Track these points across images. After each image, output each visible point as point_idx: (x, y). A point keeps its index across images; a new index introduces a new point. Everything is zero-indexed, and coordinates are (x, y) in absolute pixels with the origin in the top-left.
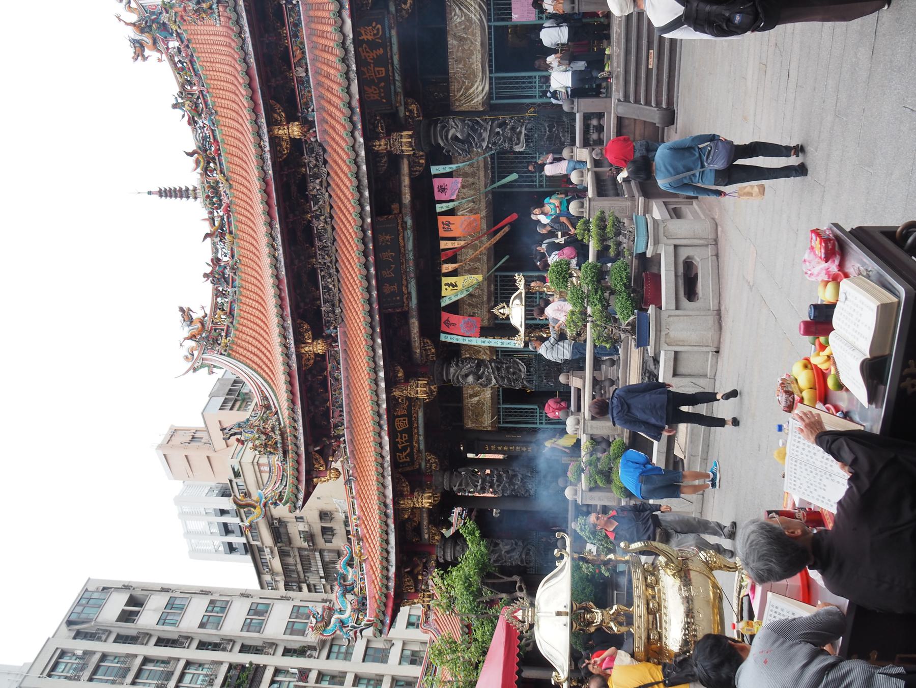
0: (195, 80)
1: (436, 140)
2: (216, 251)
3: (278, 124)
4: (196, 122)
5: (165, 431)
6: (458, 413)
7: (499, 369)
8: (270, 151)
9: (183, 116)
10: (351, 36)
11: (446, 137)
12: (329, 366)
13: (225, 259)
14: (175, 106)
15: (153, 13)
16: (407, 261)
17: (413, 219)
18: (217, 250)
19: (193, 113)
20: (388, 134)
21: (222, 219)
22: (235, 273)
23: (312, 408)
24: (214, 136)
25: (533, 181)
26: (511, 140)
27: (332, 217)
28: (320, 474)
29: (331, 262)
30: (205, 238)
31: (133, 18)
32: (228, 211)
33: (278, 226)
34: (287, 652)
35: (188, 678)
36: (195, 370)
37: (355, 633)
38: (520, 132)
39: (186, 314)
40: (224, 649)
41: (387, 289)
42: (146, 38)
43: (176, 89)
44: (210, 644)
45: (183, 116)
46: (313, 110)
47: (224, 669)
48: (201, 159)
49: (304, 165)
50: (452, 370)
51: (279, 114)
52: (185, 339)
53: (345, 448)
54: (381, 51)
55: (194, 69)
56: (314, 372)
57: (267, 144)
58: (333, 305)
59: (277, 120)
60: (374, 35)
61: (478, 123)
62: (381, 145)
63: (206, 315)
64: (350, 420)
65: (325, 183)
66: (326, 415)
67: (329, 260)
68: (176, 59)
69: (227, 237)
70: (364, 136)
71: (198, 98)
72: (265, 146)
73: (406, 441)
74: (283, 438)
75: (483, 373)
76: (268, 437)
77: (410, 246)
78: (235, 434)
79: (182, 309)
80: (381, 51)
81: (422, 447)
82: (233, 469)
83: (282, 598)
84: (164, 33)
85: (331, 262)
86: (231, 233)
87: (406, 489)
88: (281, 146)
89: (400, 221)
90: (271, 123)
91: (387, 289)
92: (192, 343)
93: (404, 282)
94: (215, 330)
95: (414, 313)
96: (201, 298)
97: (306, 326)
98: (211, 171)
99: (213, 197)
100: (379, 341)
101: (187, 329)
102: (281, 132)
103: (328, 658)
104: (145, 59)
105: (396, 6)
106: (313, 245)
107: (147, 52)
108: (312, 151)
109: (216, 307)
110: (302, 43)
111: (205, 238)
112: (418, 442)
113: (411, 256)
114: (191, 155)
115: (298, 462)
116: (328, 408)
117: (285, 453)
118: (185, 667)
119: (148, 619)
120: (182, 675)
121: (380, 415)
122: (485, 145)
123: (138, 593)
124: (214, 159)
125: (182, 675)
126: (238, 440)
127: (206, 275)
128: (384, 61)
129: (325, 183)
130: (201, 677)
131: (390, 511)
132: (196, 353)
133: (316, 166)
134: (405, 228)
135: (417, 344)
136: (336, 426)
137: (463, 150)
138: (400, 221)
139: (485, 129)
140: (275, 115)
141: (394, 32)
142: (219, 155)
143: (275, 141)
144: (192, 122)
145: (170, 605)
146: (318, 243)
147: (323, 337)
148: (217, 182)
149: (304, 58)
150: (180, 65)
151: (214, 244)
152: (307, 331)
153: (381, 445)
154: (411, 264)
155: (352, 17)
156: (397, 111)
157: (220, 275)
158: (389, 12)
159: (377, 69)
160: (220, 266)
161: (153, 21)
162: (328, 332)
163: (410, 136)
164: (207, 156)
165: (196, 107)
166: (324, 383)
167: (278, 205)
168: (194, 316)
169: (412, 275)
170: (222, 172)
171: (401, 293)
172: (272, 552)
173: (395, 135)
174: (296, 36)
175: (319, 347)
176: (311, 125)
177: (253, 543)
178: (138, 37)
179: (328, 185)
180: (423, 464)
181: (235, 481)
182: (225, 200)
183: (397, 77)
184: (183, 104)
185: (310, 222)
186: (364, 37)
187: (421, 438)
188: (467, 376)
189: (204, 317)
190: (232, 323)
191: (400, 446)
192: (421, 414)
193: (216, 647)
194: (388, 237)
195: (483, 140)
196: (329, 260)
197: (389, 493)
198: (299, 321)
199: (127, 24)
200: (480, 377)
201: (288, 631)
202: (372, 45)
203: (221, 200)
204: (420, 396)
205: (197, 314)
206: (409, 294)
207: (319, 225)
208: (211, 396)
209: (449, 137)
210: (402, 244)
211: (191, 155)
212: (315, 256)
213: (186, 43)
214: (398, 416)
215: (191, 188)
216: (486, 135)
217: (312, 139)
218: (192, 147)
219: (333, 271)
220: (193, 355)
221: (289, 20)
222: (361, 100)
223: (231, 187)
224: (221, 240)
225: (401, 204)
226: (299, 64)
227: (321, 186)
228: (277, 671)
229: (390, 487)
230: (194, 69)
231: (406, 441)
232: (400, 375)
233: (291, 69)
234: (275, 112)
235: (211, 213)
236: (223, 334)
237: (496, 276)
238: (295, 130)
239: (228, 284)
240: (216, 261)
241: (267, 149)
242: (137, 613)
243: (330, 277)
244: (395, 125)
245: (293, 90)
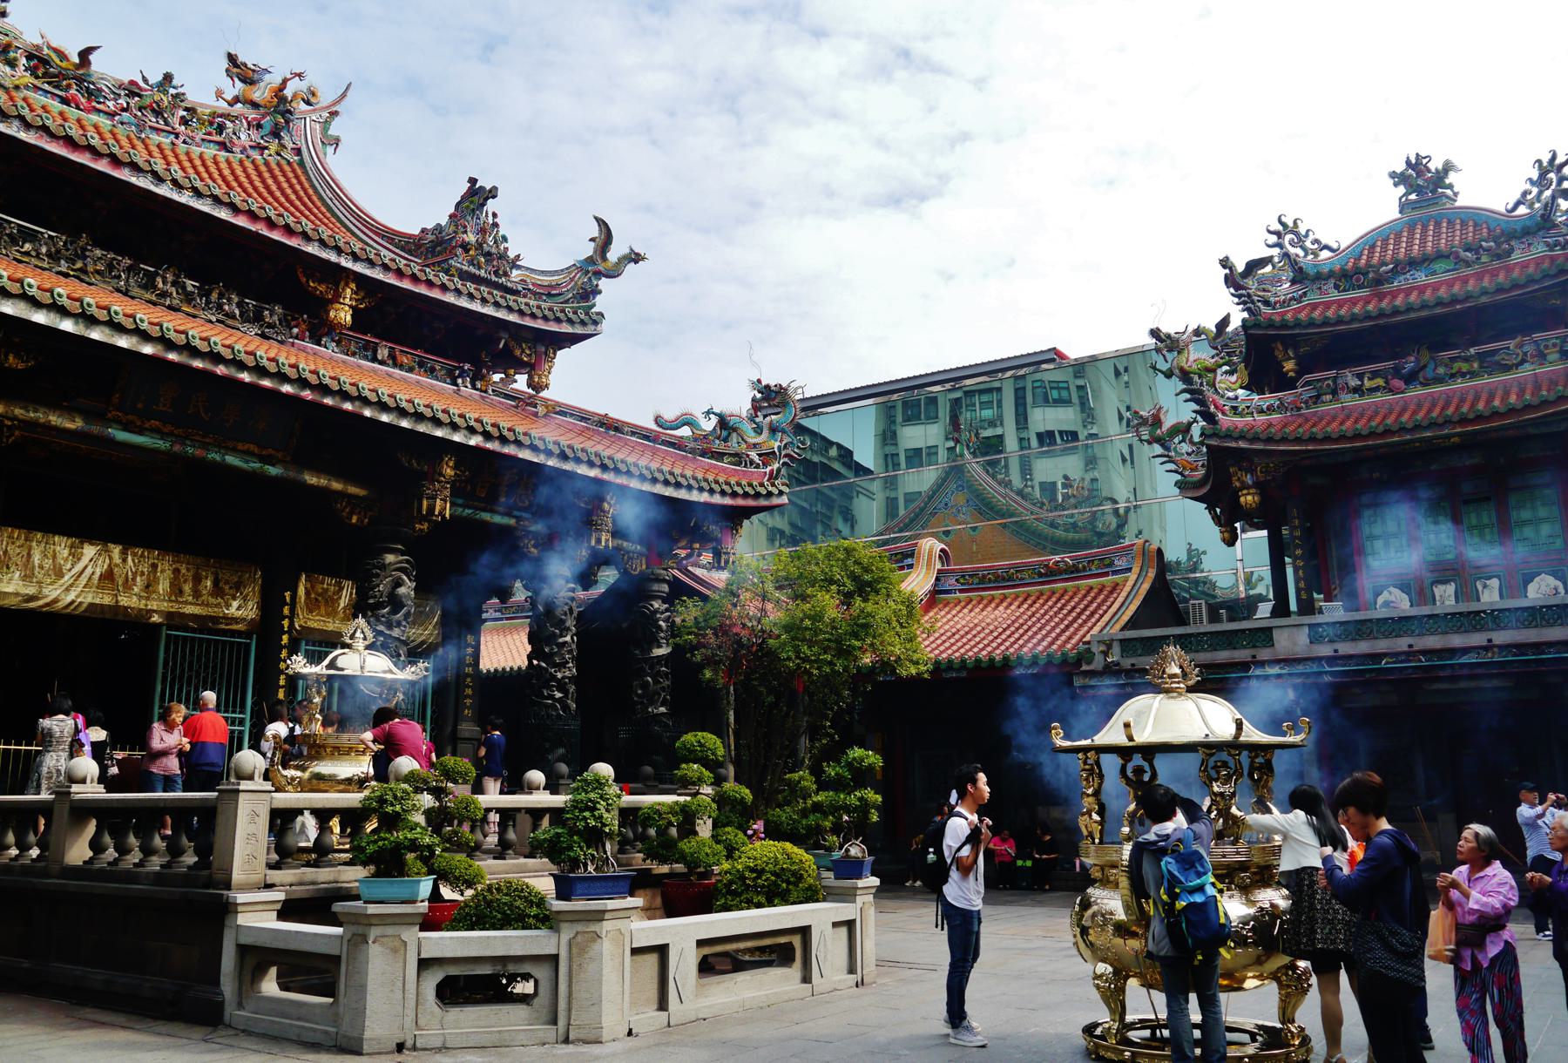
4: (131, 94)
8: (338, 266)
14: (168, 78)
16: (205, 446)
17: (276, 479)
19: (148, 101)
24: (99, 111)
25: (234, 706)
31: (288, 93)
45: (145, 80)
48: (64, 64)
67: (90, 268)
68: (229, 124)
70: (476, 448)
71: (167, 124)
77: (231, 459)
89: (279, 455)
90: (361, 279)
95: (95, 429)
100: (148, 349)
107: (239, 84)
110: (411, 370)
113: (214, 456)
114: (85, 54)
129: (230, 322)
135: (18, 412)
138: (279, 455)
141: (512, 522)
142: (65, 101)
143: (337, 275)
144: (132, 90)
148: (12, 64)
149: (395, 365)
154: (198, 452)
161: (287, 122)
165: (153, 110)
167: (256, 233)
169: (177, 448)
174: (421, 364)
184: (166, 92)
195: (390, 627)
199: (285, 81)
206: (140, 432)
210: (240, 446)
211: (85, 54)
213: (251, 152)
217: (295, 330)
218: (97, 63)
226: (392, 356)
227: (226, 315)
243: (49, 255)
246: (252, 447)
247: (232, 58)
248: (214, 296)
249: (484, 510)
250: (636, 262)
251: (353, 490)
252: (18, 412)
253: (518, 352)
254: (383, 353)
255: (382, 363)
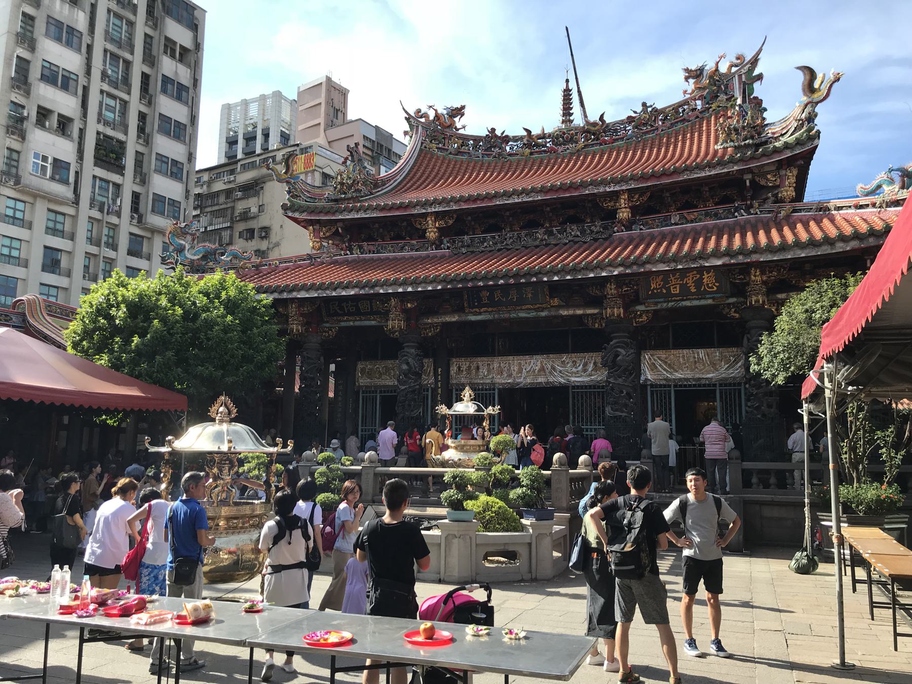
0: (668, 123)
1: (616, 338)
2: (515, 139)
3: (630, 199)
5: (344, 84)
6: (372, 356)
7: (413, 391)
9: (635, 112)
10: (707, 265)
11: (618, 347)
12: (414, 242)
13: (508, 148)
14: (644, 104)
15: (727, 86)
17: (546, 317)
18: (516, 141)
20: (621, 296)
21: (545, 146)
22: (495, 157)
23: (377, 226)
24: (617, 140)
26: (616, 403)
27: (547, 245)
28: (315, 233)
29: (507, 245)
30: (526, 130)
31: (723, 69)
32: (551, 150)
33: (540, 198)
34: (136, 197)
35: (112, 102)
36: (407, 119)
37: (172, 263)
38: (622, 412)
39: (458, 112)
40: (139, 137)
41: (485, 294)
42: (705, 81)
43: (659, 107)
44: (144, 123)
45: (635, 112)
46: (641, 229)
47: (121, 137)
49: (592, 221)
50: (413, 350)
51: (638, 200)
52: (436, 111)
53: (341, 255)
54: (693, 290)
55: (677, 122)
56: (409, 228)
57: (612, 189)
58: (468, 246)
59: (633, 197)
60: (708, 284)
61: (631, 374)
62: (611, 289)
63: (457, 130)
64: (365, 261)
65: (577, 239)
66: (370, 239)
67: (509, 243)
69: (528, 151)
71: (652, 126)
72: (610, 187)
73: (348, 310)
74: (349, 199)
75: (410, 378)
76: (350, 187)
77: (522, 315)
78: (352, 155)
79: (463, 107)
80: (693, 290)
81: (343, 324)
82: (311, 147)
83: (187, 191)
84: (708, 98)
85: (507, 245)
86: (531, 154)
87: (305, 310)
88: (610, 201)
91: (485, 294)
92: (432, 115)
93: (490, 309)
94: (444, 138)
96: (473, 125)
97: (451, 222)
98: (586, 136)
99: (563, 137)
101: (445, 112)
102: (622, 201)
103: (131, 234)
104: (687, 79)
105: (733, 304)
106: (522, 228)
107: (692, 81)
108: (605, 228)
109: (465, 138)
110: (700, 220)
111: (526, 130)
112: (348, 320)
113: (513, 315)
115: (327, 213)
116: (377, 241)
117: (336, 200)
118: (121, 99)
119: (168, 66)
120: (114, 97)
121: (373, 287)
122: (611, 380)
123: (191, 58)
124: (598, 139)
125: (114, 97)
126: (346, 159)
127: (493, 130)
128: (685, 293)
130: (112, 115)
131: (285, 295)
132: (423, 120)
133: (592, 232)
134: (537, 310)
135: (435, 320)
136: (360, 247)
137: (607, 361)
139: (625, 381)
140: (637, 196)
141: (710, 302)
142: (601, 144)
143: (616, 195)
144: (630, 119)
145: (181, 88)
146: (523, 233)
147: (441, 237)
149: (688, 222)
150: (681, 110)
151: (521, 138)
152: (446, 223)
153: (347, 287)
154: (507, 316)
155: (724, 265)
156: (641, 304)
157: (494, 141)
158: (728, 297)
159: (678, 286)
160: (502, 143)
161: (719, 87)
162: (445, 241)
163: (619, 315)
164: (599, 133)
166: (399, 237)
168: (456, 119)
169: (496, 316)
170: (586, 146)
171: (480, 307)
172: (230, 182)
173: (619, 301)
174: (707, 215)
175: (432, 235)
176: (629, 228)
177: (239, 164)
178: (705, 73)
179: (576, 243)
180: (327, 325)
181: (298, 149)
182: (560, 149)
183: (670, 304)
185: (542, 226)
186: (706, 276)
187: (351, 323)
188: (408, 364)
189: (456, 128)
190: (450, 153)
191: (344, 304)
192: (373, 323)
193: (141, 130)
194: (530, 295)
195: (616, 379)
196: (509, 243)
197: (303, 295)
198: (455, 216)
200: (406, 375)
201: (156, 197)
202: (699, 283)
203: (560, 145)
204: (390, 323)
205: (459, 122)
206: (480, 314)
207: (540, 234)
208: (377, 128)
209: (619, 350)
210: (523, 307)
212: (512, 231)
214: (371, 303)
215: (571, 118)
216: (620, 381)
218: (608, 119)
219: (499, 246)
220: (421, 117)
221: (721, 209)
222: (651, 273)
223: (572, 154)
224: (524, 144)
225: (559, 307)
226: (682, 217)
228: (118, 186)
229: (307, 296)
230: (677, 122)
231: (348, 310)
232: (409, 305)
233: (678, 210)
234: (640, 196)
235: (550, 136)
236: (440, 145)
237: (494, 390)
238: (624, 214)
239: (485, 150)
240: (506, 139)
241: (608, 190)
242: (173, 56)
244: (630, 301)
245: (659, 212)
246: (529, 306)
247: (687, 70)
248: (569, 230)
249: (683, 300)
250: (839, 79)
251: (589, 311)
252: (435, 320)
253: (763, 183)
254: (675, 218)
255: (676, 224)
